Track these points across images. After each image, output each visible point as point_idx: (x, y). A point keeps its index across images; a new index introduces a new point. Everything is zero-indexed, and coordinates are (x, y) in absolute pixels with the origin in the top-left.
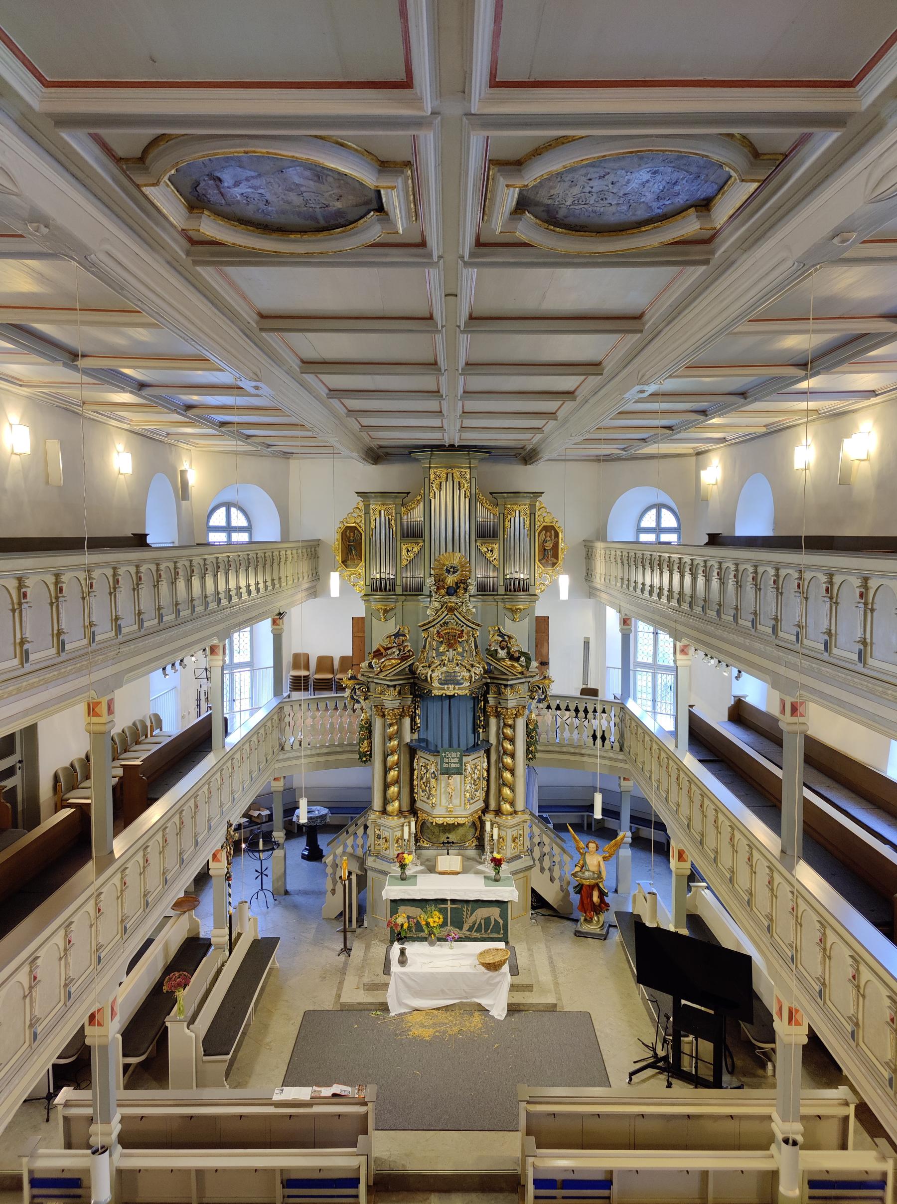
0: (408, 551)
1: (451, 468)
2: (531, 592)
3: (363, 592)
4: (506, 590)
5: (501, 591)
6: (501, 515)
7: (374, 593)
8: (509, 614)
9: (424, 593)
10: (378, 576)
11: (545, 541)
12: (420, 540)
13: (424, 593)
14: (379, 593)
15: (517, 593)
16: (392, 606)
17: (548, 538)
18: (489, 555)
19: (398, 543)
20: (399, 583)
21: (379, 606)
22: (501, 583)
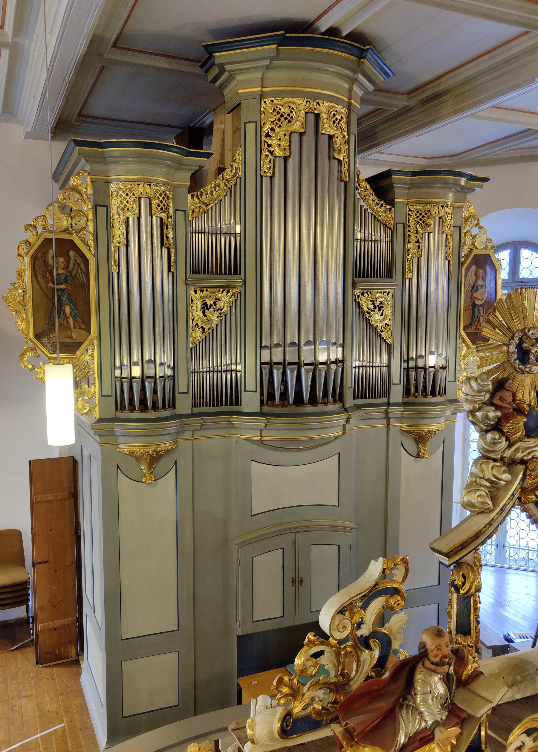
0: (205, 307)
1: (317, 98)
2: (449, 395)
3: (96, 414)
4: (407, 392)
5: (397, 394)
6: (400, 228)
7: (127, 414)
8: (410, 444)
9: (245, 408)
10: (136, 372)
11: (475, 288)
12: (236, 281)
13: (245, 408)
14: (137, 415)
15: (421, 399)
16: (167, 445)
17: (480, 282)
18: (376, 316)
19: (181, 287)
20: (182, 386)
21: (137, 448)
22: (396, 376)
